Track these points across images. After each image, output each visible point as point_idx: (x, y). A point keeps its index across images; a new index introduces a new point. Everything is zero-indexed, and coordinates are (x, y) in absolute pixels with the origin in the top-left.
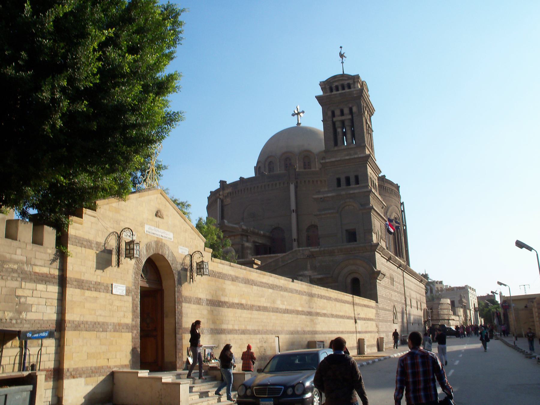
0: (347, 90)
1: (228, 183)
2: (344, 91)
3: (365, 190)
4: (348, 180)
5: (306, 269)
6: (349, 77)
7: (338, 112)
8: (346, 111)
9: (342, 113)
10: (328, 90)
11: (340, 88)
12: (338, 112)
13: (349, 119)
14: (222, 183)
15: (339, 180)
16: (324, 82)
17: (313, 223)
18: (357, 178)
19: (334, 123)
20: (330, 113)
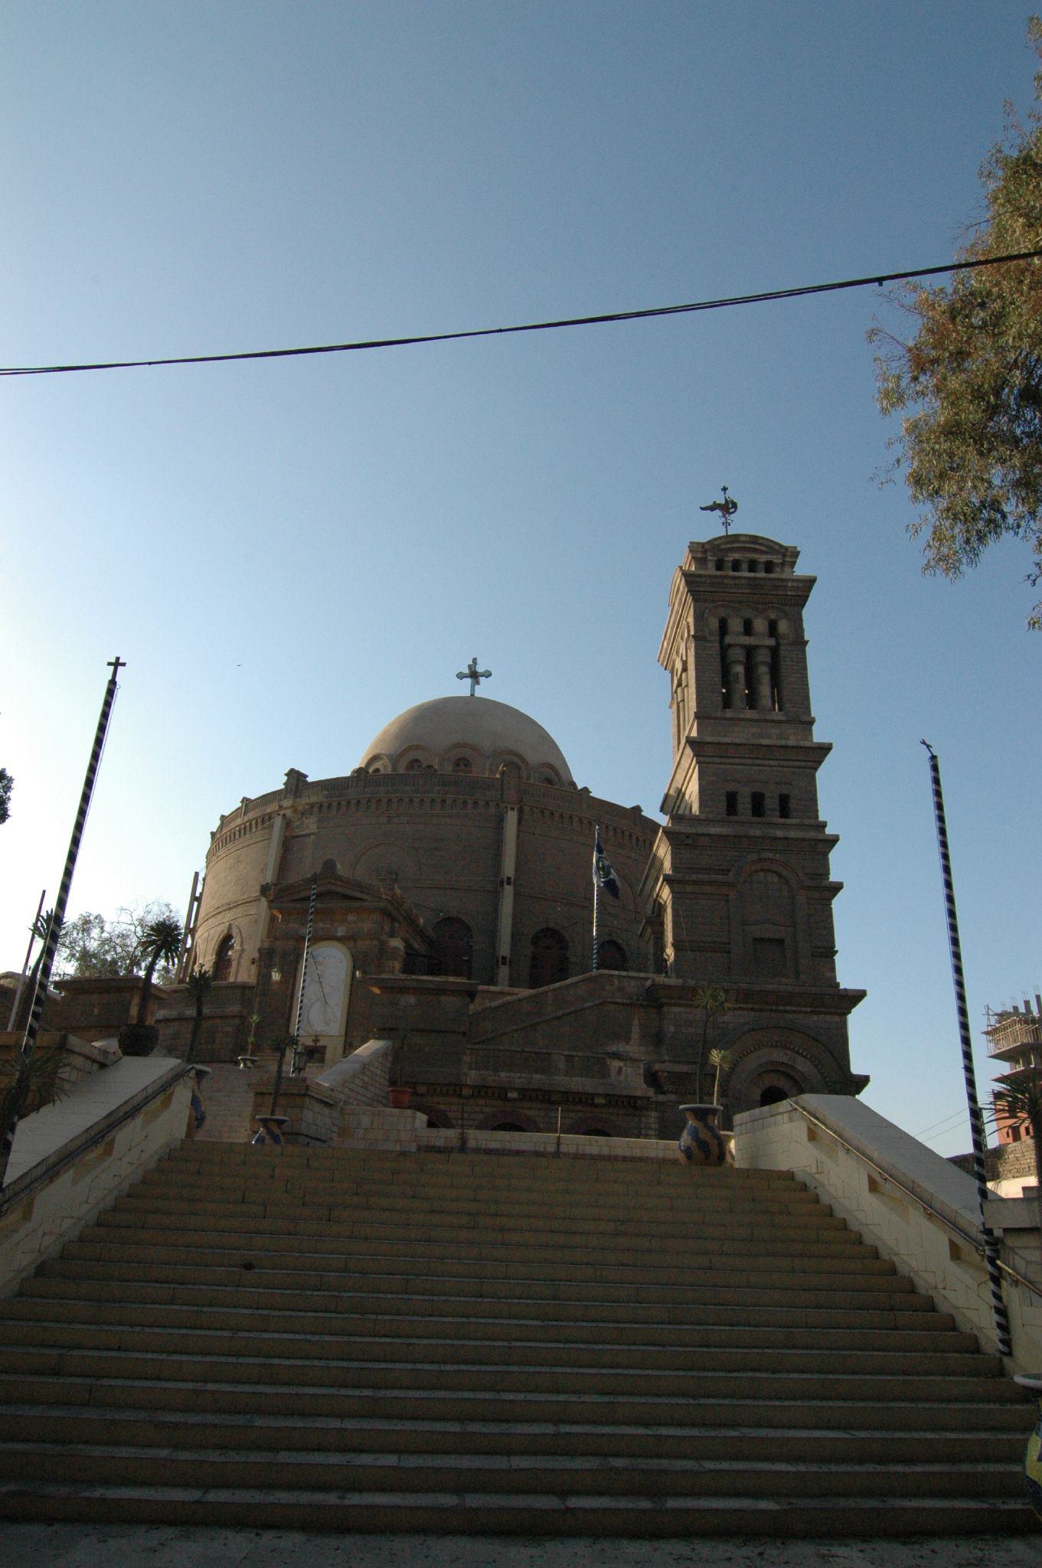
0: (762, 575)
1: (309, 780)
2: (752, 575)
3: (812, 835)
4: (758, 801)
5: (627, 1039)
6: (772, 547)
7: (736, 624)
8: (760, 625)
9: (748, 629)
10: (711, 565)
11: (745, 566)
12: (736, 624)
13: (770, 648)
14: (296, 778)
15: (732, 799)
16: (703, 545)
17: (551, 925)
18: (784, 800)
19: (724, 650)
20: (714, 624)
